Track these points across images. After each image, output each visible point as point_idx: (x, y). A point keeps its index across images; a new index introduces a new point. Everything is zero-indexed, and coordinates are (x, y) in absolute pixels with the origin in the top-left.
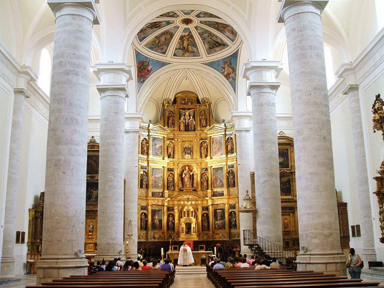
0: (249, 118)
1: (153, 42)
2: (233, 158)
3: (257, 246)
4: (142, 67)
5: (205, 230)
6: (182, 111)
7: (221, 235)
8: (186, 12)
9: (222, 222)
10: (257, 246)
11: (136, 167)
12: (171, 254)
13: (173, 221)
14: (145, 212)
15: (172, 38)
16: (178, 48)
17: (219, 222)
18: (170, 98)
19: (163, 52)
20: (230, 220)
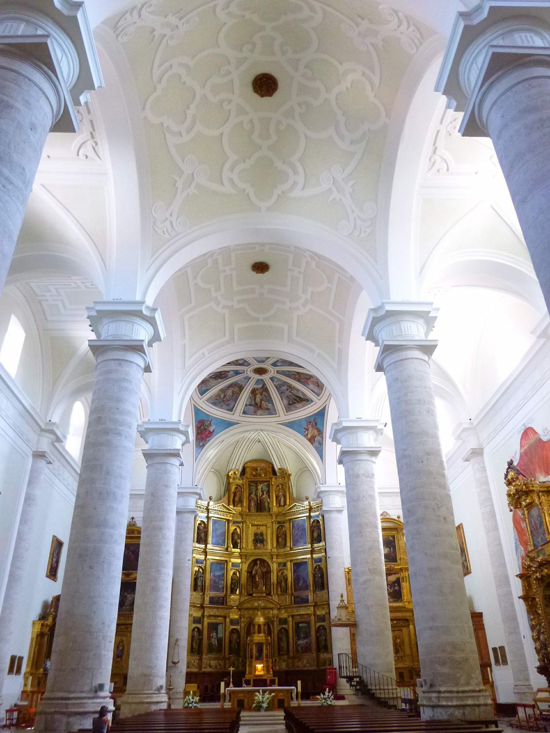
0: (340, 494)
1: (217, 396)
2: (320, 549)
3: (358, 679)
4: (202, 427)
5: (284, 655)
7: (305, 661)
8: (259, 359)
9: (307, 642)
10: (358, 679)
11: (189, 560)
12: (234, 692)
14: (199, 626)
15: (241, 391)
16: (248, 403)
19: (229, 408)
20: (317, 638)
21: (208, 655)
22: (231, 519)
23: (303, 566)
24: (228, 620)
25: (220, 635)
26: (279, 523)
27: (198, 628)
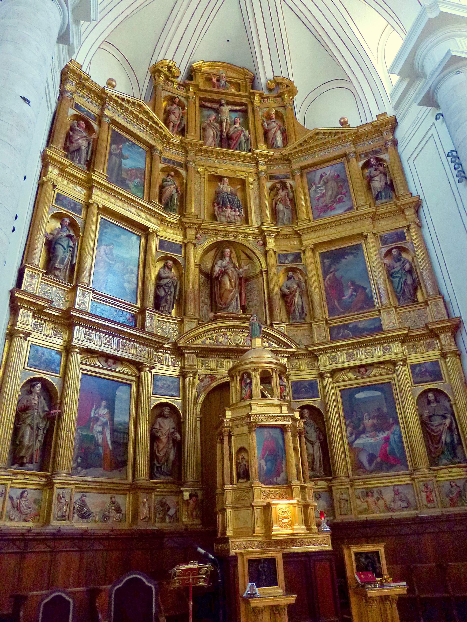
6: (208, 105)
9: (387, 439)
13: (178, 436)
17: (372, 440)
18: (177, 60)
21: (77, 474)
22: (159, 147)
23: (350, 258)
24: (146, 376)
25: (120, 418)
26: (272, 178)
27: (46, 386)
